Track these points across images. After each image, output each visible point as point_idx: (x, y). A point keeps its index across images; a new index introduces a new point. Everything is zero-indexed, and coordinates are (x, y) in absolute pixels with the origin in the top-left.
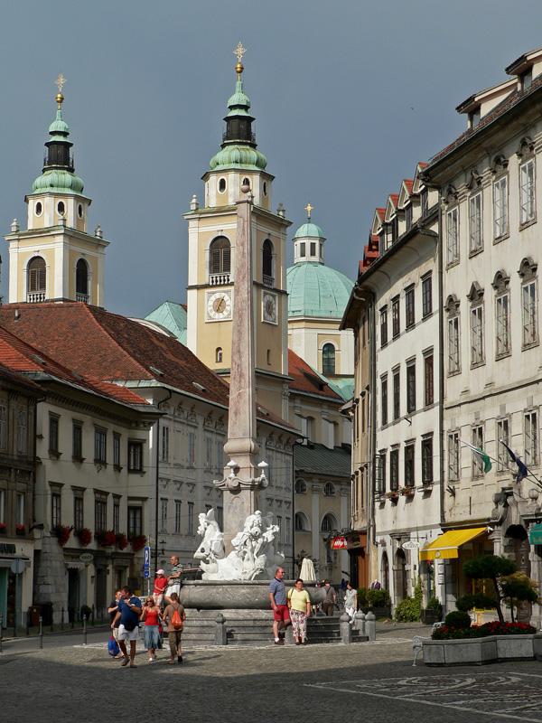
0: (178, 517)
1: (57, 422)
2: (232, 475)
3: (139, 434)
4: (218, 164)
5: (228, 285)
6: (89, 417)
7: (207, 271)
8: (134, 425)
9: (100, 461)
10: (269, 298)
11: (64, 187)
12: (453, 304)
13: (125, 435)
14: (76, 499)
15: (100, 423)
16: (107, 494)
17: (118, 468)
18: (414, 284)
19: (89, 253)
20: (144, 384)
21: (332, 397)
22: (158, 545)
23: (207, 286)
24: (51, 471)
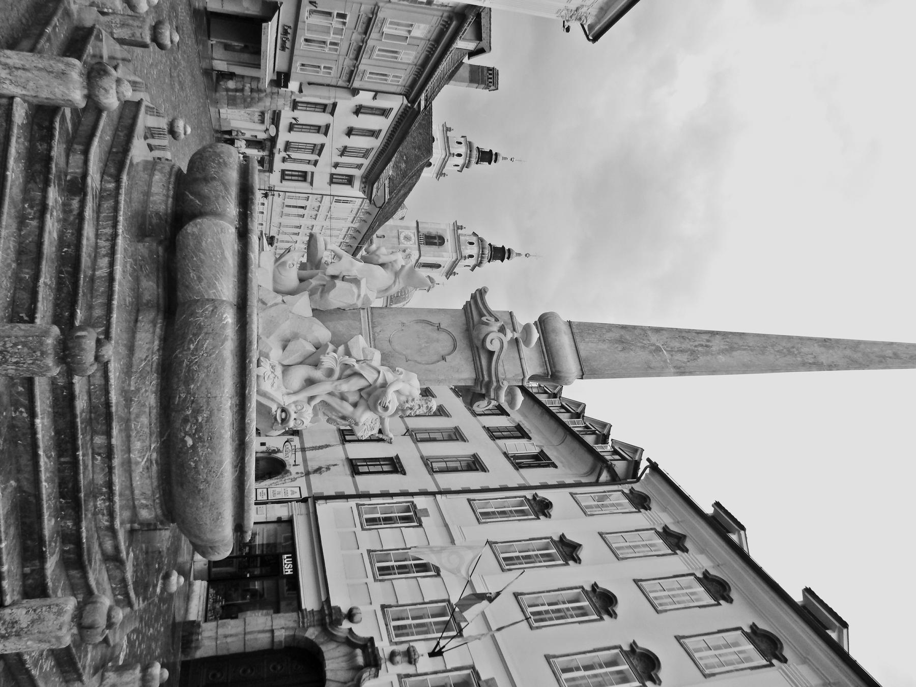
1: (382, 115)
2: (510, 335)
3: (357, 183)
5: (419, 243)
8: (364, 180)
9: (344, 151)
12: (543, 508)
13: (358, 173)
14: (319, 127)
15: (372, 155)
16: (319, 155)
17: (336, 165)
18: (530, 438)
22: (278, 192)
24: (346, 104)
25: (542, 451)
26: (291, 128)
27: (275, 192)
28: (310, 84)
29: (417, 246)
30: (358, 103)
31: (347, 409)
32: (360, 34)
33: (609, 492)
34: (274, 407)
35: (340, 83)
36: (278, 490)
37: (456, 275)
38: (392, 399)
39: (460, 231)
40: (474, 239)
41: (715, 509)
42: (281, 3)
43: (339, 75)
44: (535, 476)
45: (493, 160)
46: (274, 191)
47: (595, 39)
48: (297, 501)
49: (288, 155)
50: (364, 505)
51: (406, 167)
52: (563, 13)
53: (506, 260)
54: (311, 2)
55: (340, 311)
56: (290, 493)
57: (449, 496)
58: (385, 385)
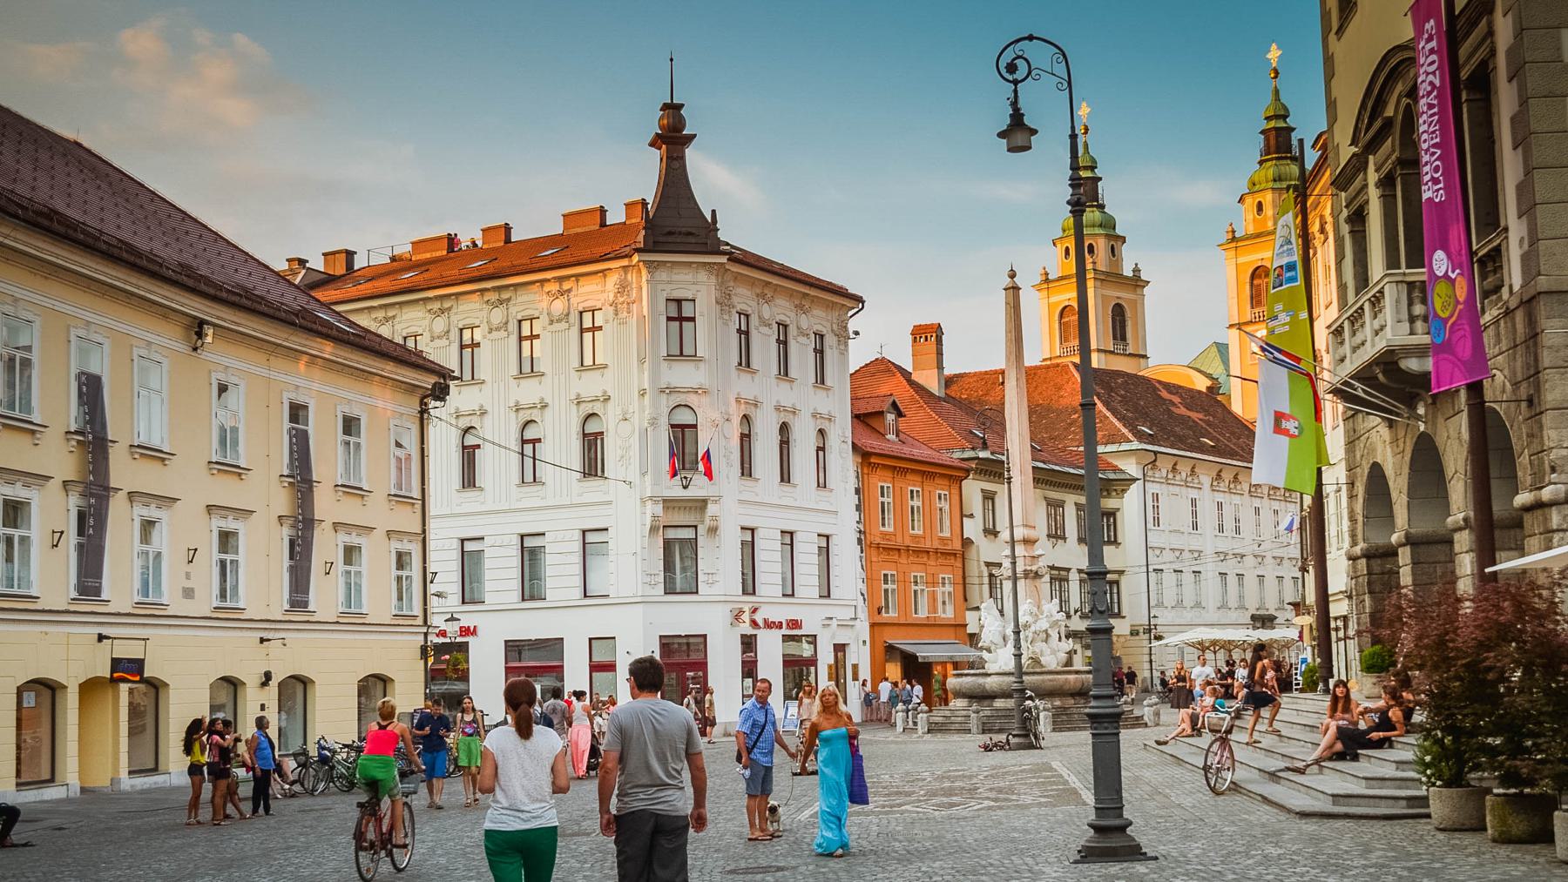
11: (1094, 226)
15: (1055, 495)
16: (1068, 570)
19: (1124, 295)
20: (1125, 447)
27: (1153, 621)
28: (966, 600)
30: (982, 534)
35: (959, 565)
42: (886, 642)
46: (1150, 625)
47: (859, 300)
49: (1076, 612)
54: (879, 613)
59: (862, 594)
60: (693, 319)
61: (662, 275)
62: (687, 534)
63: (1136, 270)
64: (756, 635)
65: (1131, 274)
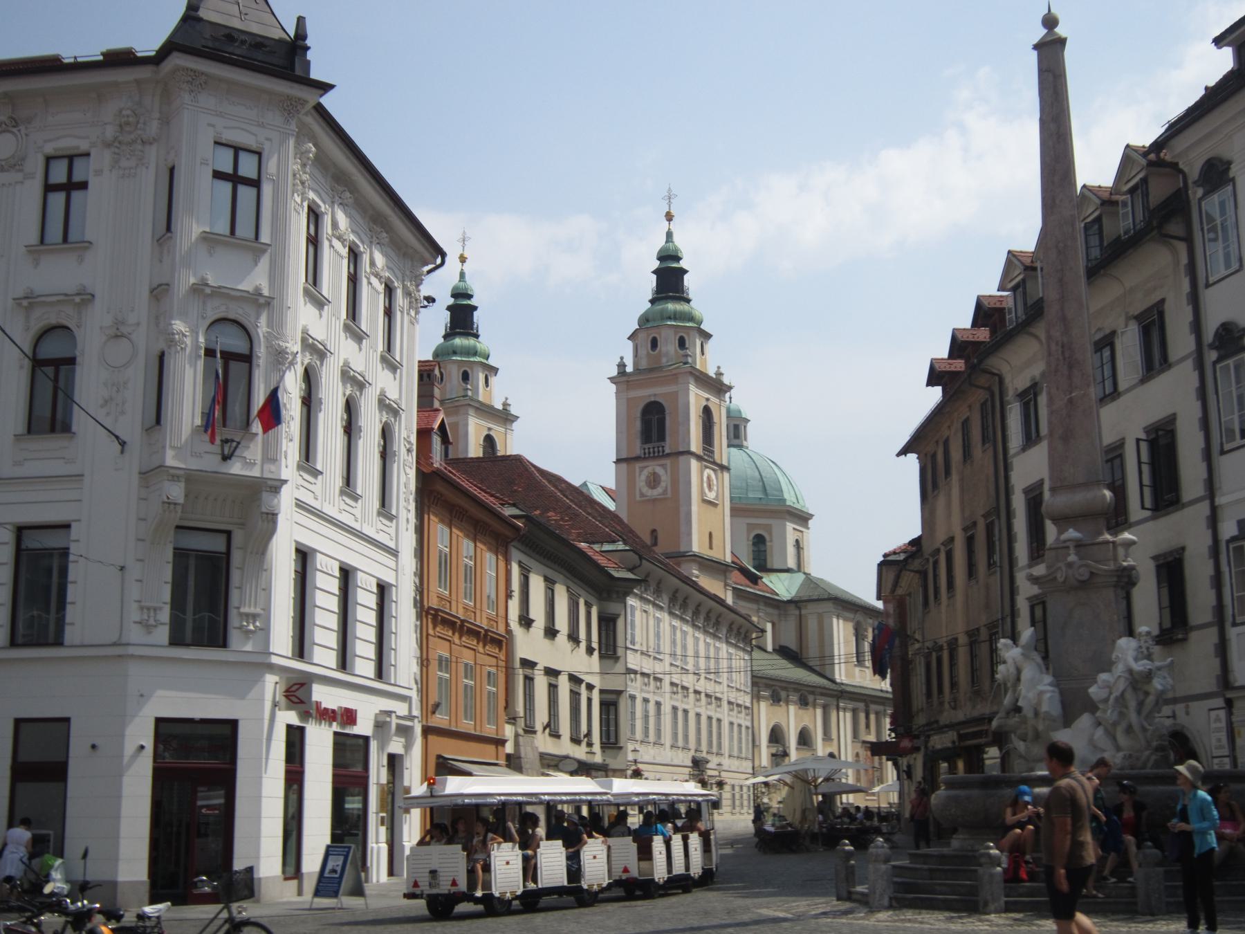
0: (646, 717)
2: (1072, 558)
3: (613, 607)
4: (648, 321)
6: (561, 576)
7: (638, 442)
10: (707, 472)
17: (590, 651)
18: (1113, 333)
19: (497, 431)
20: (607, 547)
21: (768, 593)
23: (637, 459)
25: (1136, 318)
26: (556, 735)
29: (668, 462)
31: (1151, 699)
32: (453, 634)
33: (1201, 223)
34: (1153, 758)
36: (1214, 742)
37: (722, 370)
38: (1140, 666)
39: (629, 369)
40: (645, 339)
41: (1228, 45)
43: (494, 660)
44: (1180, 341)
45: (469, 302)
48: (1230, 714)
49: (585, 736)
50: (1234, 616)
51: (554, 510)
52: (413, 313)
53: (683, 264)
54: (434, 713)
55: (1064, 705)
56: (1218, 725)
57: (1217, 485)
58: (1130, 671)
59: (416, 683)
60: (256, 184)
61: (207, 100)
62: (218, 544)
63: (505, 405)
64: (301, 730)
65: (500, 407)
